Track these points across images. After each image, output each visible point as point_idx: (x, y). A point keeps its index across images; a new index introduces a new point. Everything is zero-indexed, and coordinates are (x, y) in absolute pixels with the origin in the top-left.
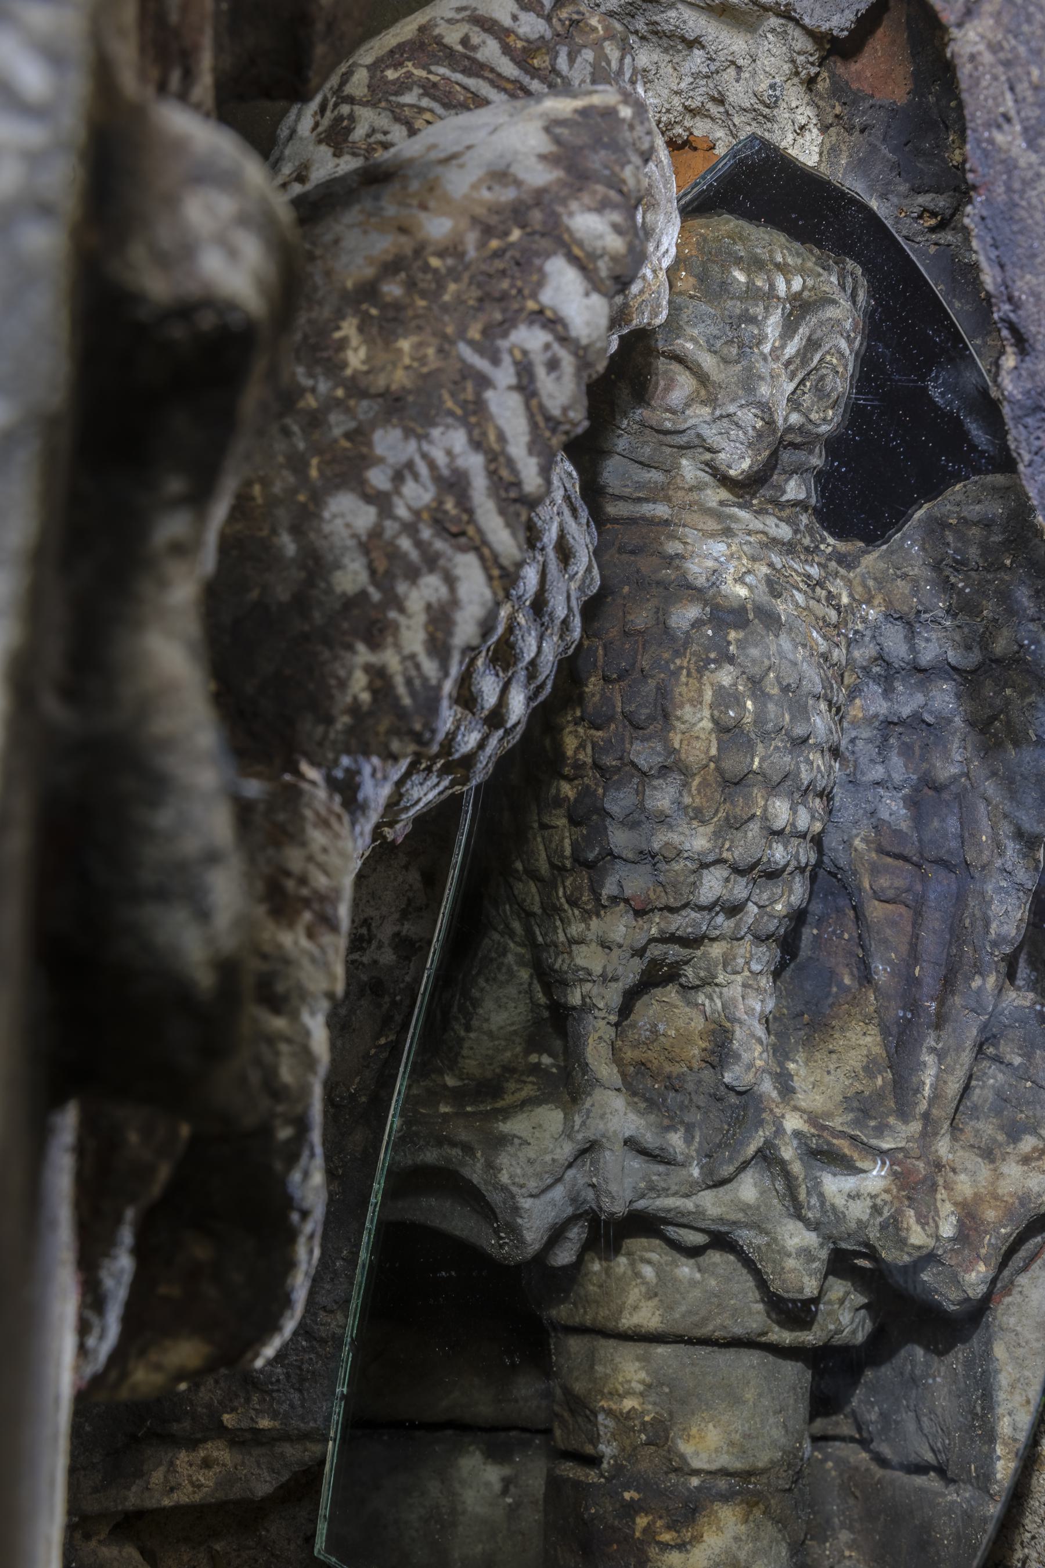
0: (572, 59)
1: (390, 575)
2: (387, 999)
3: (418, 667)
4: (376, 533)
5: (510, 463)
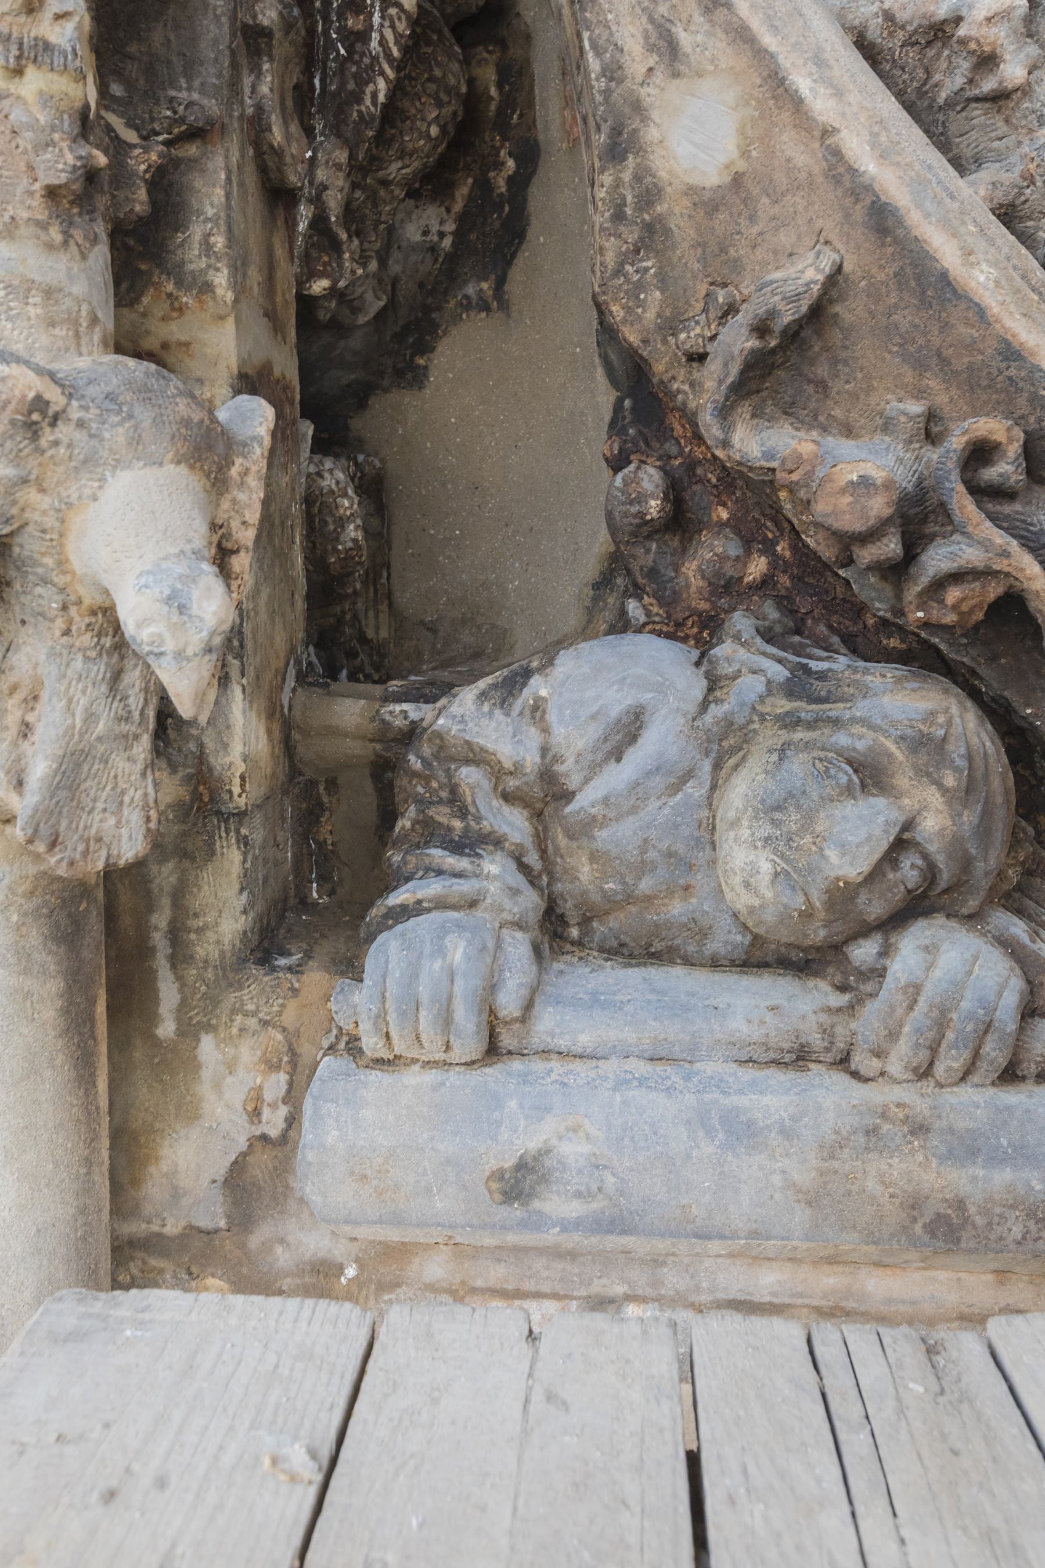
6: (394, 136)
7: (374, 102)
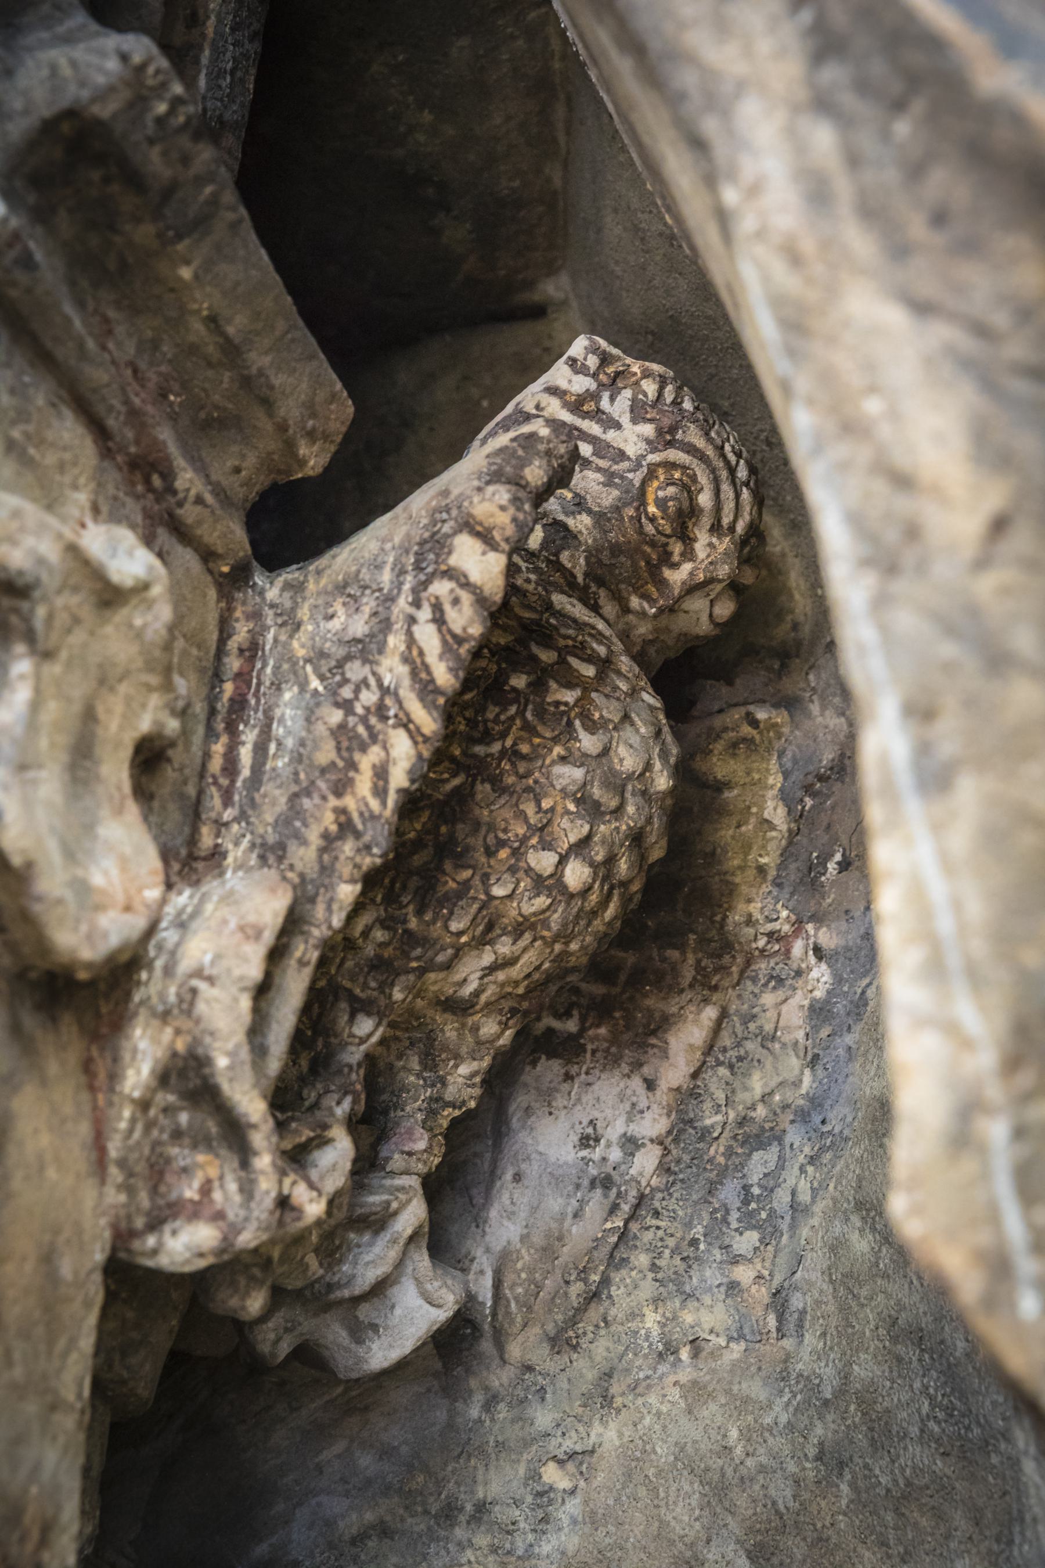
0: (612, 399)
1: (349, 749)
2: (614, 1190)
3: (367, 805)
4: (342, 726)
5: (427, 668)
6: (466, 885)
7: (380, 792)
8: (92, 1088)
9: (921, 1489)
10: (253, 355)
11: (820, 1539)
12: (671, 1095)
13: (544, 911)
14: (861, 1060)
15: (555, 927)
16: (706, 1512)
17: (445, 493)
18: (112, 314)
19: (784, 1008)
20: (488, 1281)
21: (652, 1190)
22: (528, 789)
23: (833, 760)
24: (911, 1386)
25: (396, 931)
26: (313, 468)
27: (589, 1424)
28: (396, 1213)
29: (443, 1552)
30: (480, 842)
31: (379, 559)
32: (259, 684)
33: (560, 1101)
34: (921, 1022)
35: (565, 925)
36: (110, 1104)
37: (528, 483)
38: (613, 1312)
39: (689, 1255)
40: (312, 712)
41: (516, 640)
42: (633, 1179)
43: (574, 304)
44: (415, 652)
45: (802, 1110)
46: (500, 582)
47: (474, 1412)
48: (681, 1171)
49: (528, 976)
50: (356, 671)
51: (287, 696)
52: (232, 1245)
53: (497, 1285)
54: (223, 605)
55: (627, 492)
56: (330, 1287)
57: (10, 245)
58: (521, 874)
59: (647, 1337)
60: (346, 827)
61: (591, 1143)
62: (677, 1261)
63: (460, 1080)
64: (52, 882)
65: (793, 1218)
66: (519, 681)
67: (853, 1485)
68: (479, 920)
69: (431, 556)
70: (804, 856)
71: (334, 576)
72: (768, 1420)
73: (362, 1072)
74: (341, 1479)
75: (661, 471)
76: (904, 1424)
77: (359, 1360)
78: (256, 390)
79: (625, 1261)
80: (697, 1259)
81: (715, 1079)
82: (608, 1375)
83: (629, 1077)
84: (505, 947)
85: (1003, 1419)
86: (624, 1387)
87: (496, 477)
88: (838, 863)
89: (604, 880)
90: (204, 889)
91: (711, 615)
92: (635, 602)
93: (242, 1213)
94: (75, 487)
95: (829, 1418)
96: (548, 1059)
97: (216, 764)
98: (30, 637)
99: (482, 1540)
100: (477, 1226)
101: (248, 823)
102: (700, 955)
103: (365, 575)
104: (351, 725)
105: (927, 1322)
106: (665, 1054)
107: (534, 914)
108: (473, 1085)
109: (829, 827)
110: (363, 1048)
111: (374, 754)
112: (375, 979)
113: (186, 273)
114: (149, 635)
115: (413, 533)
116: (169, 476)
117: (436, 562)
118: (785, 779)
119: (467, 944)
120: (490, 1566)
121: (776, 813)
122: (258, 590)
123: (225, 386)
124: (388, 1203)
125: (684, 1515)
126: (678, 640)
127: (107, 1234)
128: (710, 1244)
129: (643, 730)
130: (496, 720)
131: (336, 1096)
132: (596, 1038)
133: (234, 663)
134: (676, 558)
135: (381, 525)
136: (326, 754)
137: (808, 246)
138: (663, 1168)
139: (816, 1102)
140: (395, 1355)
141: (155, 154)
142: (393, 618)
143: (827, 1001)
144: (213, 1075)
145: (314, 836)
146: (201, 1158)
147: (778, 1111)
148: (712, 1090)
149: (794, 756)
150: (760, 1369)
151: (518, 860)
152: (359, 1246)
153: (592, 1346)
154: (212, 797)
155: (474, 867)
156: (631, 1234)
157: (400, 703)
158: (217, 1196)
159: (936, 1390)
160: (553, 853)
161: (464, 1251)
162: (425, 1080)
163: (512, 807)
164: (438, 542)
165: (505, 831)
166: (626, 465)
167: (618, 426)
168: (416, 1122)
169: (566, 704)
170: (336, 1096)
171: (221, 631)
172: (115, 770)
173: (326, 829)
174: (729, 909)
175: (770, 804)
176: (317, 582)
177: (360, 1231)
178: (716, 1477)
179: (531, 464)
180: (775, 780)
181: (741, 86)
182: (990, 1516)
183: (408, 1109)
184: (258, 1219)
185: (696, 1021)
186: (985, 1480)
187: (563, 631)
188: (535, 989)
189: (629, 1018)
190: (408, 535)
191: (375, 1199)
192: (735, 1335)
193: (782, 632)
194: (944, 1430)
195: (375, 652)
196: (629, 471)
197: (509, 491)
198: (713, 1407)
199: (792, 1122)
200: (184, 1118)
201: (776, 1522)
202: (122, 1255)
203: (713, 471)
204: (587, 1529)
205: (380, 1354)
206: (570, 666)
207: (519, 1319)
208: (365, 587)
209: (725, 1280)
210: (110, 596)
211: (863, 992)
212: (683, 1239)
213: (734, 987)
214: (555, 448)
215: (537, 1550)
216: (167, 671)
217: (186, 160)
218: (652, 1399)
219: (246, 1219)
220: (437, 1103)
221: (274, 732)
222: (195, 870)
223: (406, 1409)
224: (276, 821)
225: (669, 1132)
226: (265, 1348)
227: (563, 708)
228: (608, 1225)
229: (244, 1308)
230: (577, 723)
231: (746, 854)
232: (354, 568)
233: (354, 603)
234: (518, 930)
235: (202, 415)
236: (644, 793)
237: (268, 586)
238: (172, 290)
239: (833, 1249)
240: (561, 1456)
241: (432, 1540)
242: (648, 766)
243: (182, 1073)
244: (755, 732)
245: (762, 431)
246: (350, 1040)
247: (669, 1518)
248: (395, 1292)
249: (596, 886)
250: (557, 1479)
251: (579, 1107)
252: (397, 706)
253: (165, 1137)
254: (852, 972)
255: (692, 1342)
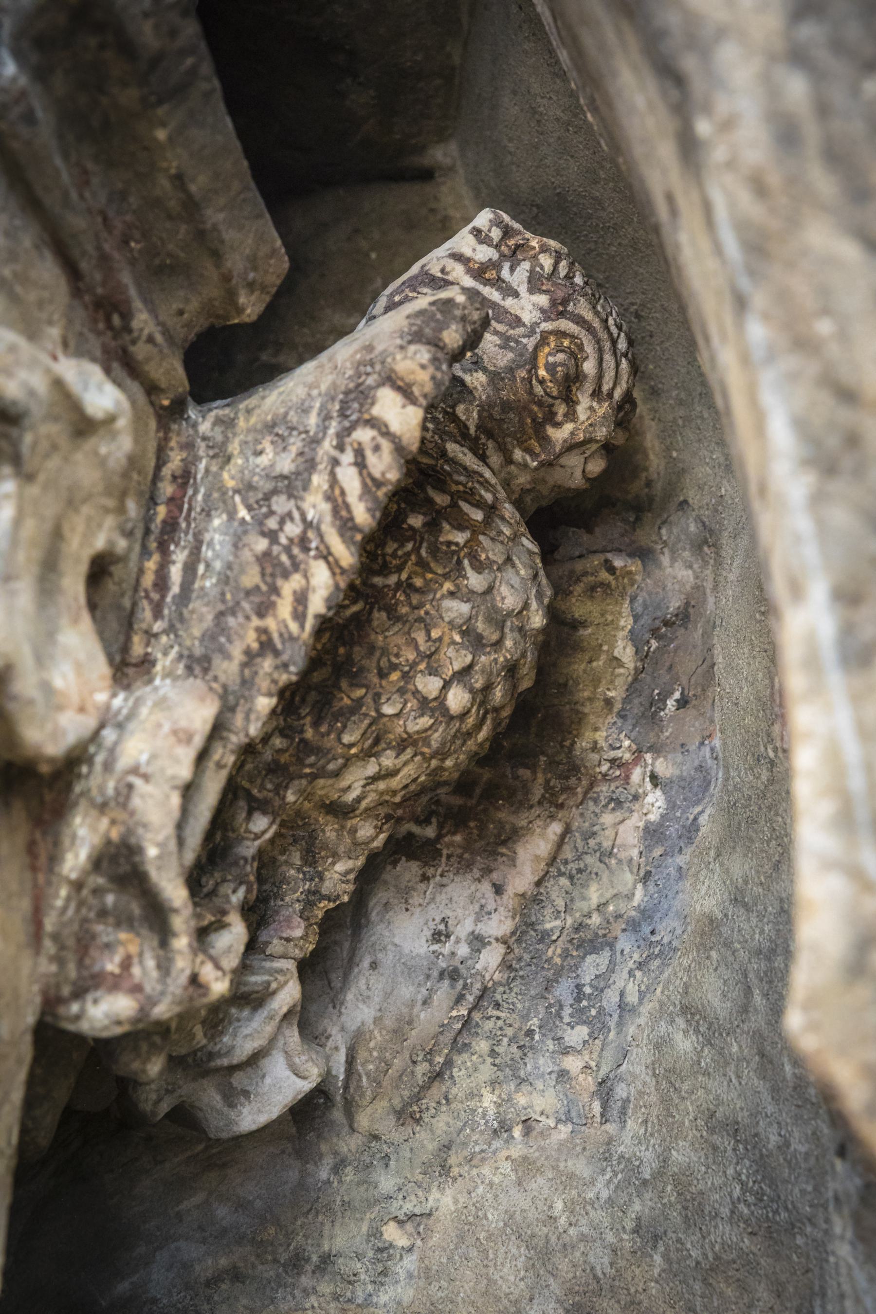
0: (512, 270)
1: (273, 575)
2: (461, 982)
3: (286, 627)
4: (267, 554)
6: (359, 703)
7: (299, 616)
8: (34, 869)
9: (728, 1263)
10: (209, 212)
11: (632, 1303)
12: (516, 899)
13: (426, 730)
14: (691, 880)
15: (435, 745)
16: (531, 1274)
17: (369, 348)
18: (90, 165)
19: (621, 828)
20: (341, 1057)
21: (495, 983)
22: (420, 620)
23: (679, 608)
24: (725, 1172)
25: (293, 739)
26: (249, 316)
27: (428, 1190)
28: (274, 993)
29: (289, 1297)
30: (374, 665)
31: (306, 404)
32: (190, 510)
33: (416, 899)
34: (829, 865)
35: (443, 744)
36: (49, 883)
37: (445, 345)
38: (454, 1091)
39: (525, 1043)
40: (240, 539)
41: (414, 483)
42: (478, 973)
43: (461, 171)
44: (337, 492)
45: (634, 921)
46: (417, 434)
47: (324, 1174)
48: (521, 968)
49: (406, 786)
50: (281, 504)
51: (216, 522)
52: (147, 1015)
53: (351, 1061)
54: (161, 435)
55: (521, 355)
56: (211, 1056)
57: (17, 101)
58: (409, 696)
59: (484, 1116)
60: (266, 645)
61: (443, 938)
62: (514, 1049)
63: (336, 876)
64: (26, 685)
65: (620, 1017)
66: (416, 521)
67: (666, 1257)
68: (368, 735)
69: (356, 405)
70: (647, 692)
71: (263, 416)
72: (591, 1195)
73: (255, 864)
74: (199, 1227)
75: (552, 338)
76: (717, 1206)
77: (230, 1123)
78: (207, 243)
79: (467, 1046)
80: (532, 1048)
81: (556, 887)
82: (447, 1147)
83: (480, 881)
84: (388, 760)
85: (810, 1206)
86: (461, 1159)
87: (417, 337)
88: (677, 701)
89: (480, 706)
90: (138, 693)
91: (584, 471)
92: (518, 454)
93: (159, 987)
94: (50, 323)
95: (647, 1196)
96: (407, 861)
97: (148, 580)
98: (16, 460)
99: (326, 1288)
100: (334, 1007)
101: (177, 636)
102: (549, 775)
103: (293, 417)
104: (275, 553)
105: (743, 1116)
106: (513, 862)
107: (418, 732)
108: (348, 882)
109: (671, 668)
110: (257, 843)
111: (296, 581)
112: (271, 781)
113: (161, 135)
114: (112, 463)
115: (338, 382)
116: (127, 316)
117: (360, 411)
118: (635, 622)
119: (356, 756)
120: (332, 1311)
121: (625, 652)
122: (192, 422)
123: (180, 237)
124: (269, 983)
125: (510, 1273)
126: (552, 490)
127: (38, 1000)
128: (544, 1035)
129: (522, 572)
130: (394, 555)
131: (232, 885)
132: (451, 844)
133: (167, 489)
134: (559, 418)
135: (308, 370)
136: (251, 578)
137: (774, 180)
138: (506, 965)
139: (646, 914)
140: (263, 1119)
141: (148, 27)
142: (318, 459)
143: (661, 824)
144: (143, 863)
145: (237, 652)
146: (123, 936)
147: (612, 920)
148: (553, 897)
149: (644, 601)
150: (584, 1149)
151: (407, 683)
152: (238, 1020)
153: (434, 1121)
154: (143, 610)
155: (367, 687)
156: (474, 1023)
157: (321, 536)
158: (136, 971)
159: (748, 1177)
160: (437, 679)
161: (321, 1029)
162: (304, 874)
163: (404, 634)
164: (362, 392)
165: (397, 656)
166: (521, 330)
167: (516, 294)
168: (295, 912)
169: (457, 544)
170: (232, 885)
171: (158, 458)
172: (73, 584)
173: (248, 647)
174: (577, 736)
175: (620, 644)
176: (247, 420)
177: (241, 1007)
178: (541, 1243)
179: (448, 327)
180: (626, 622)
181: (722, 33)
182: (791, 1289)
183: (287, 899)
184: (173, 994)
185: (542, 835)
186: (789, 1258)
187: (456, 477)
188: (409, 799)
189: (482, 828)
190: (334, 385)
191: (256, 979)
192: (563, 1118)
193: (636, 487)
194: (753, 1213)
195: (300, 488)
196: (524, 336)
197: (429, 351)
198: (541, 1180)
199: (624, 930)
200: (110, 899)
201: (593, 1285)
202: (49, 1019)
203: (598, 342)
204: (422, 1283)
205: (249, 1118)
206: (462, 510)
207: (369, 1093)
208: (292, 429)
209: (556, 1068)
210: (85, 427)
211: (695, 819)
212: (520, 1029)
213: (578, 807)
214: (470, 314)
215: (375, 1299)
216: (123, 495)
217: (173, 33)
218: (486, 1170)
219: (163, 993)
220: (312, 898)
221: (203, 554)
222: (127, 675)
223: (262, 1168)
224: (203, 635)
225: (513, 933)
226: (148, 1107)
227: (453, 548)
228: (454, 1013)
229: (144, 1071)
230: (466, 562)
231: (596, 687)
232: (282, 410)
233: (281, 443)
234: (402, 745)
235: (157, 261)
236: (521, 629)
237: (200, 419)
238: (146, 148)
239: (657, 1046)
240: (401, 1217)
241: (280, 1286)
242: (526, 606)
243: (114, 859)
244: (611, 578)
245: (633, 304)
246: (247, 835)
247: (496, 1277)
248: (265, 1062)
249: (474, 710)
250: (397, 1237)
251: (433, 906)
252: (318, 540)
253: (92, 915)
254: (685, 799)
255: (524, 1122)
